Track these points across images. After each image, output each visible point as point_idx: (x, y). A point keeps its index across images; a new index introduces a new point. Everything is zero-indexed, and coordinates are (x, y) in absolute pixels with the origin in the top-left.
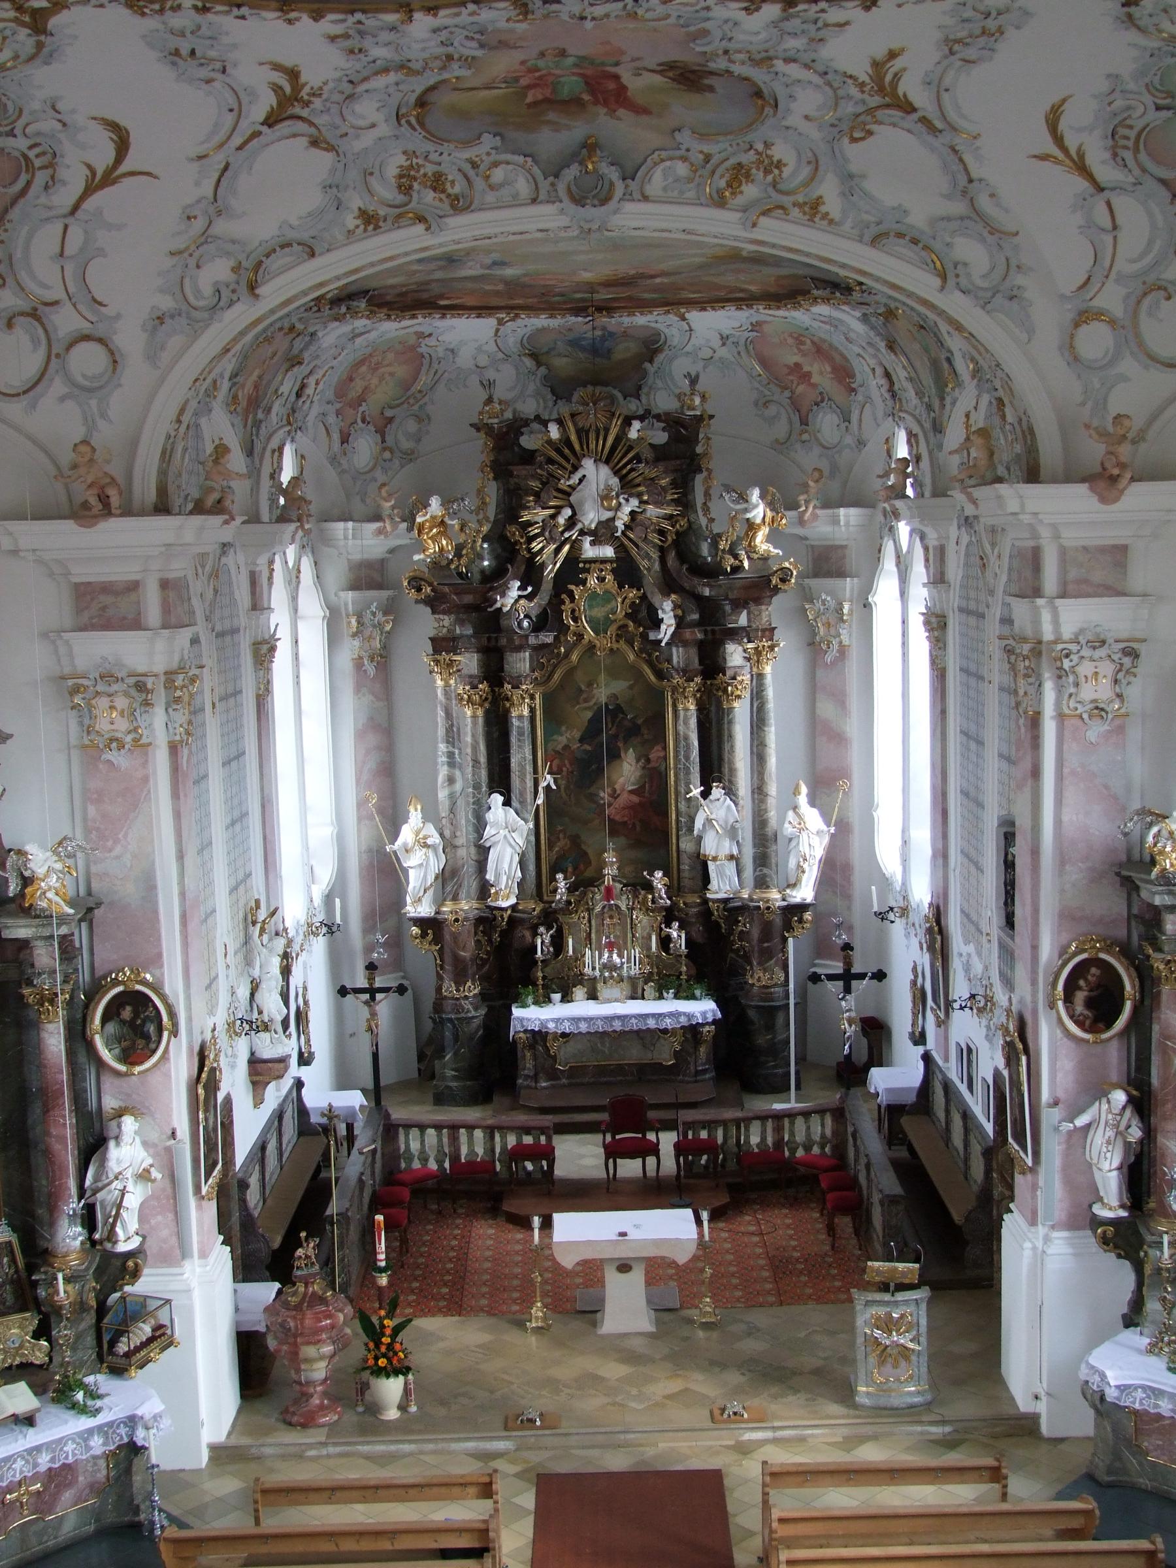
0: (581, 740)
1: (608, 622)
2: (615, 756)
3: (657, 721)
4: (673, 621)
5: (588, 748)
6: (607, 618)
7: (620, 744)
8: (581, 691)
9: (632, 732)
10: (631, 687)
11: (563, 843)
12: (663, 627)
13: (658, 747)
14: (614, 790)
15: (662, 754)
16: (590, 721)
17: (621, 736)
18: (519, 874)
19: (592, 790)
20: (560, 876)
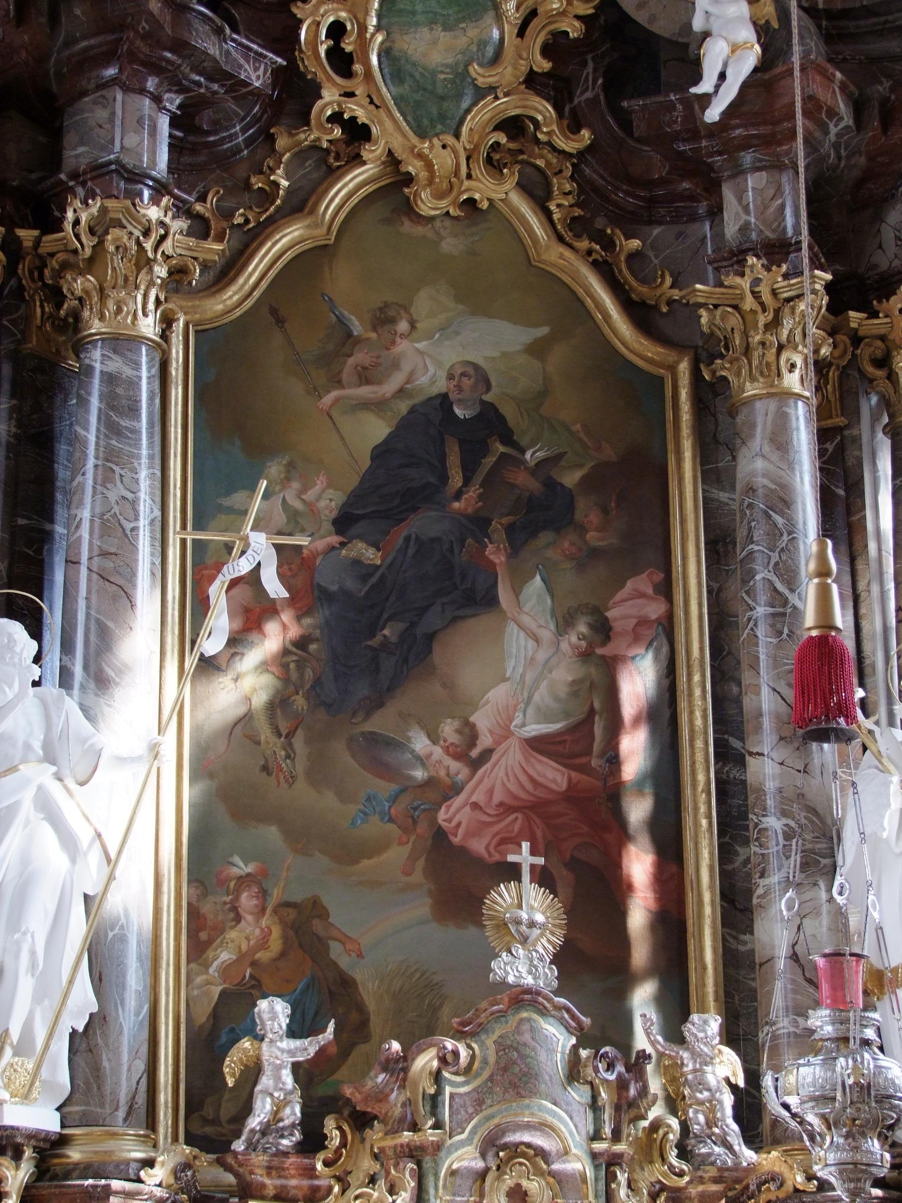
0: (344, 523)
1: (462, 87)
2: (479, 598)
3: (638, 483)
4: (747, 34)
5: (371, 555)
6: (461, 75)
7: (496, 555)
8: (347, 339)
9: (541, 514)
10: (537, 350)
11: (250, 934)
12: (714, 55)
13: (643, 583)
14: (471, 734)
15: (655, 610)
16: (380, 453)
17: (497, 526)
18: (83, 1000)
19: (381, 723)
20: (274, 1012)
